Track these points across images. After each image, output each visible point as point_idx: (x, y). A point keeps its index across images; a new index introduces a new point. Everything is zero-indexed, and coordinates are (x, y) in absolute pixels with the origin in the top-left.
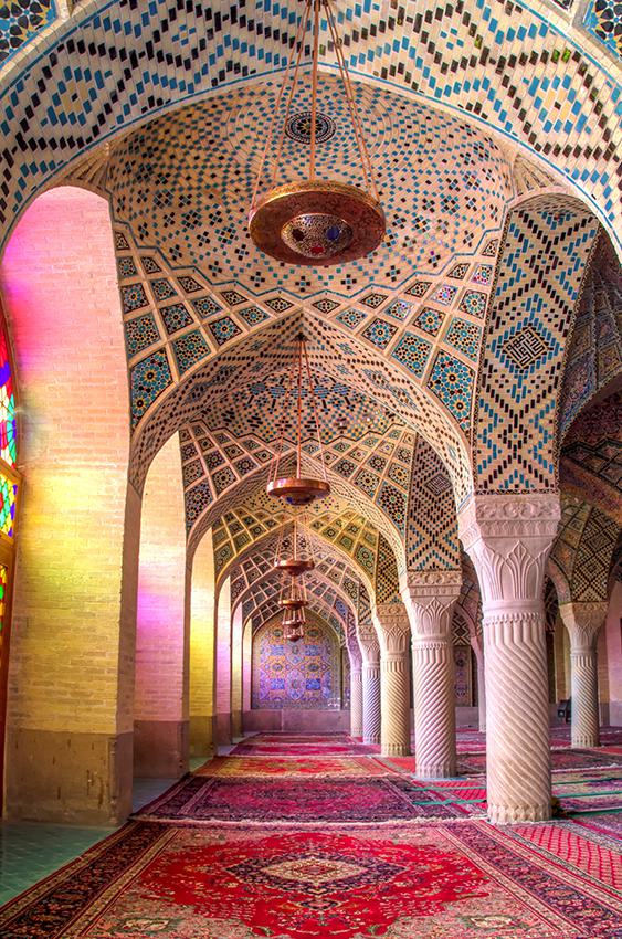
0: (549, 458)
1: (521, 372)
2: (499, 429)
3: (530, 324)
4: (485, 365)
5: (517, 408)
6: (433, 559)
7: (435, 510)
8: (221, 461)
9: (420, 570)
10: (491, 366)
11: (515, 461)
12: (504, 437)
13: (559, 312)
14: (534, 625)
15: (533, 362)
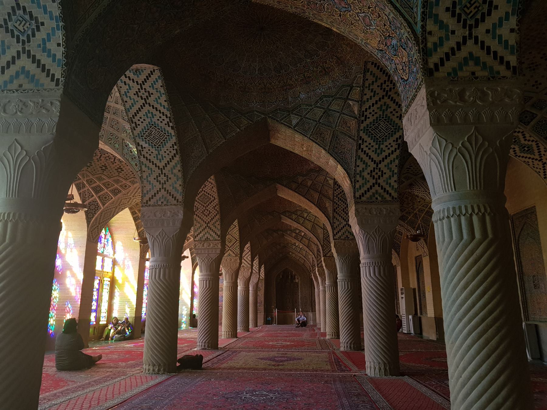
0: (180, 189)
1: (158, 147)
2: (154, 175)
3: (152, 125)
4: (139, 145)
5: (161, 165)
6: (207, 235)
7: (206, 211)
8: (102, 190)
9: (200, 240)
10: (142, 146)
11: (163, 190)
12: (156, 179)
13: (164, 117)
14: (167, 270)
15: (162, 143)
